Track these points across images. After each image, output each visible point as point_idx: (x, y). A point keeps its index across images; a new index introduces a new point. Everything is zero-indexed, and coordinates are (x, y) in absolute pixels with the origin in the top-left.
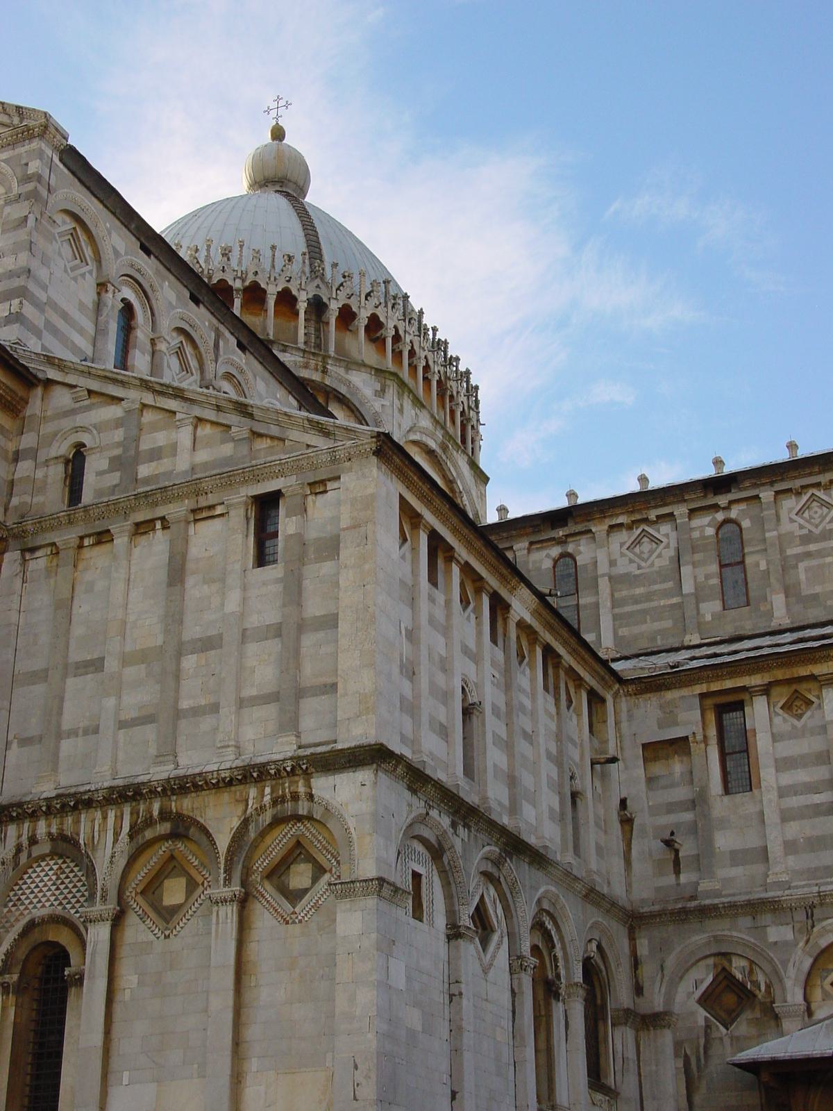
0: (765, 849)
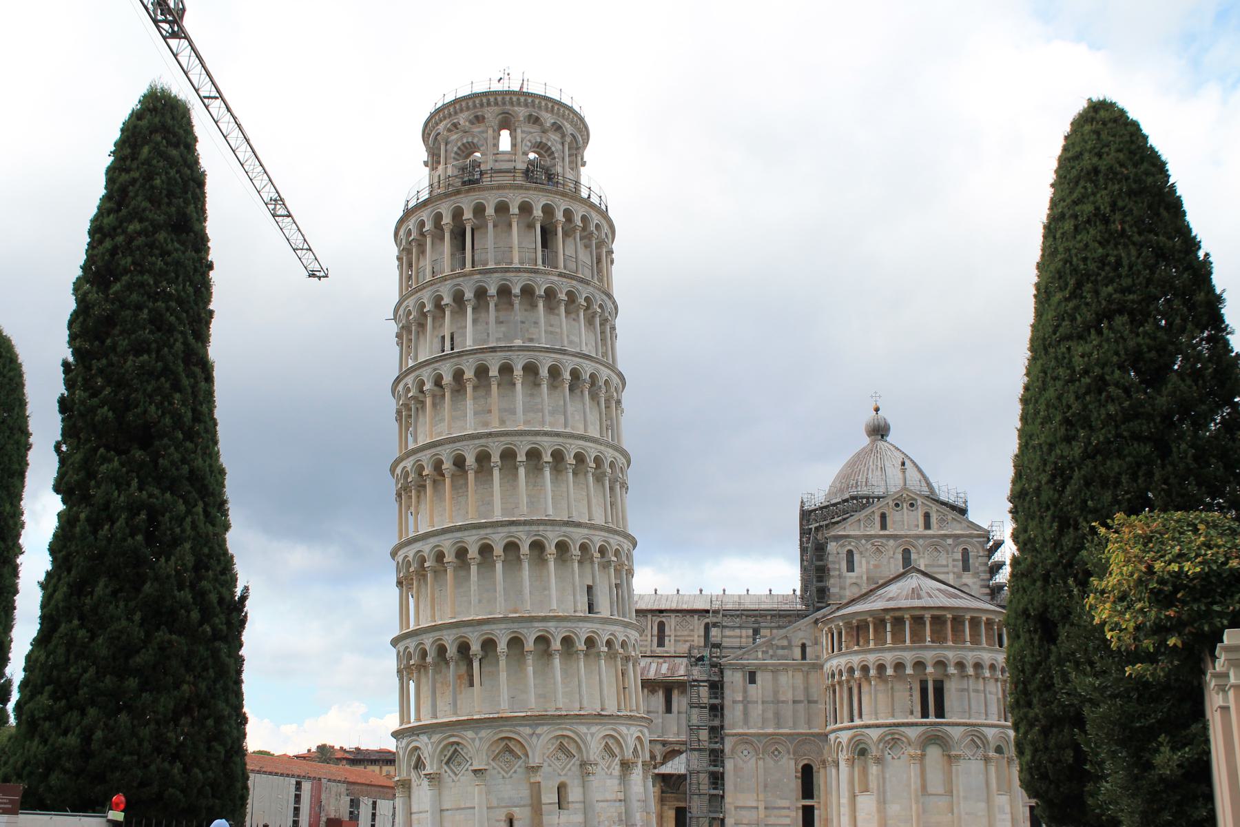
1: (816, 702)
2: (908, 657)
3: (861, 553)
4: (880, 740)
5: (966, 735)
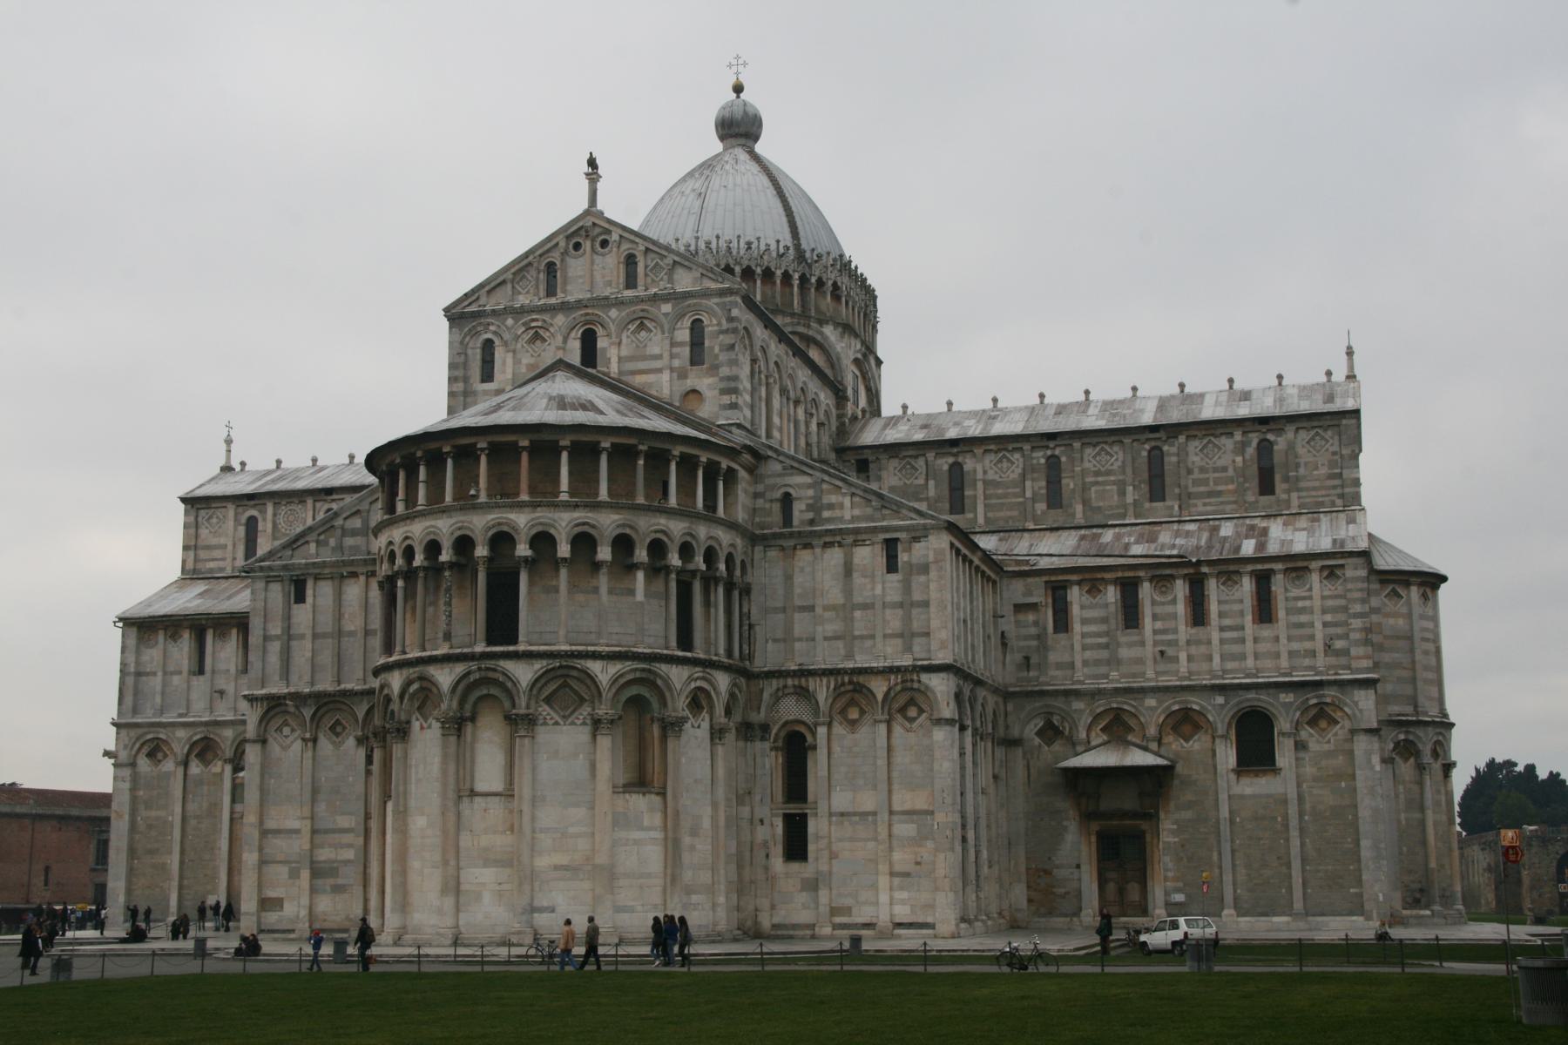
0: (1073, 662)
2: (444, 527)
3: (505, 344)
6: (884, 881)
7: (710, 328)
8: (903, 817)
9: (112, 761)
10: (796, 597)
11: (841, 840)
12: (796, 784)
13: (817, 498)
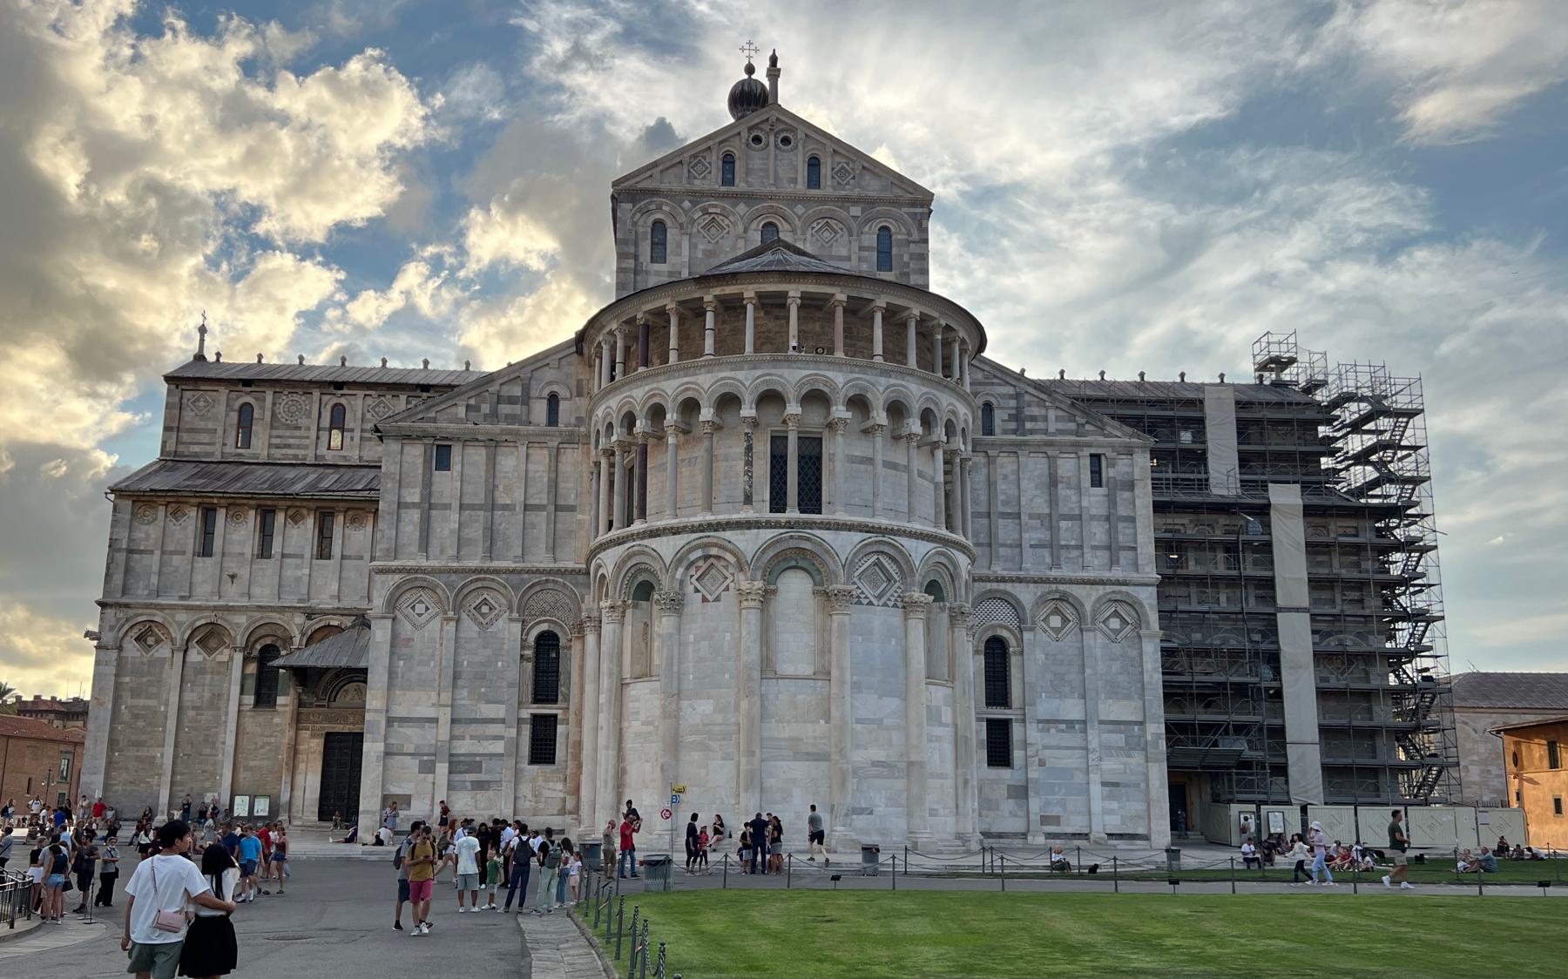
1: (572, 509)
2: (747, 379)
3: (681, 226)
4: (680, 561)
5: (863, 551)
6: (1096, 790)
7: (899, 237)
8: (1111, 727)
9: (95, 643)
10: (999, 503)
11: (1046, 747)
12: (997, 686)
13: (1019, 409)
